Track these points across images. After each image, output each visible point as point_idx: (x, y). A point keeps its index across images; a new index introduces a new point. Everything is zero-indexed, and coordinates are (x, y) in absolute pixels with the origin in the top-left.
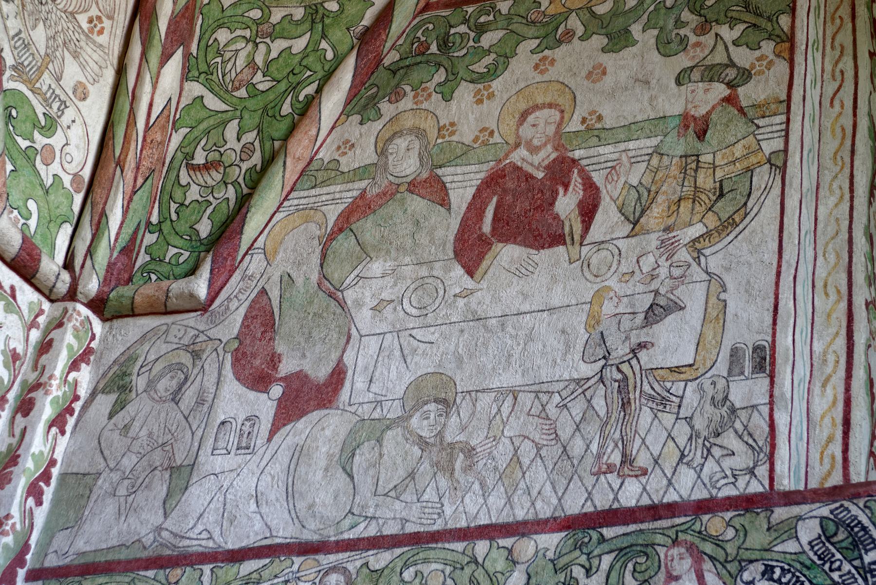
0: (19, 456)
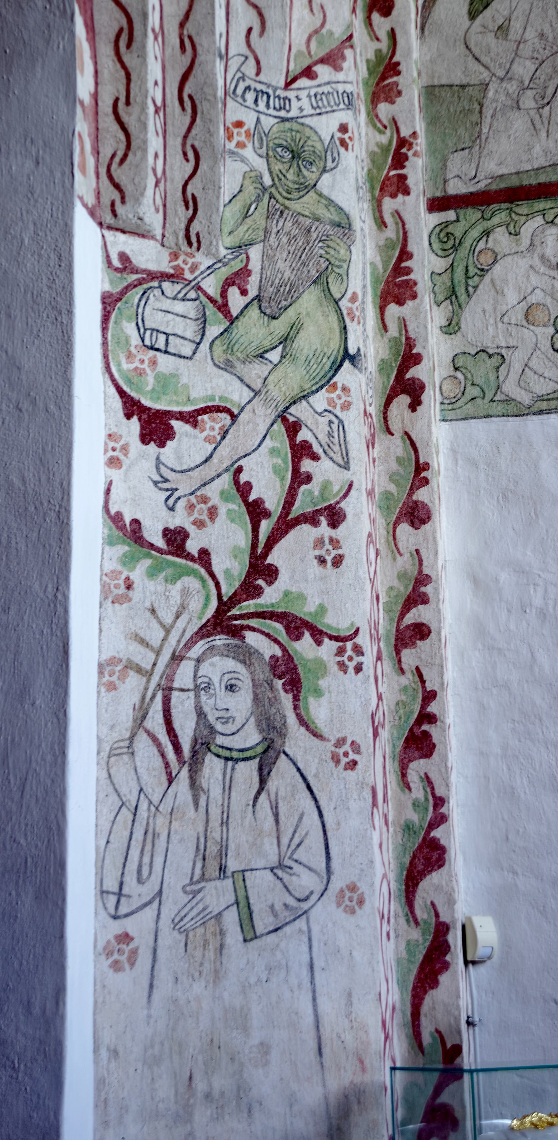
0: (398, 64)
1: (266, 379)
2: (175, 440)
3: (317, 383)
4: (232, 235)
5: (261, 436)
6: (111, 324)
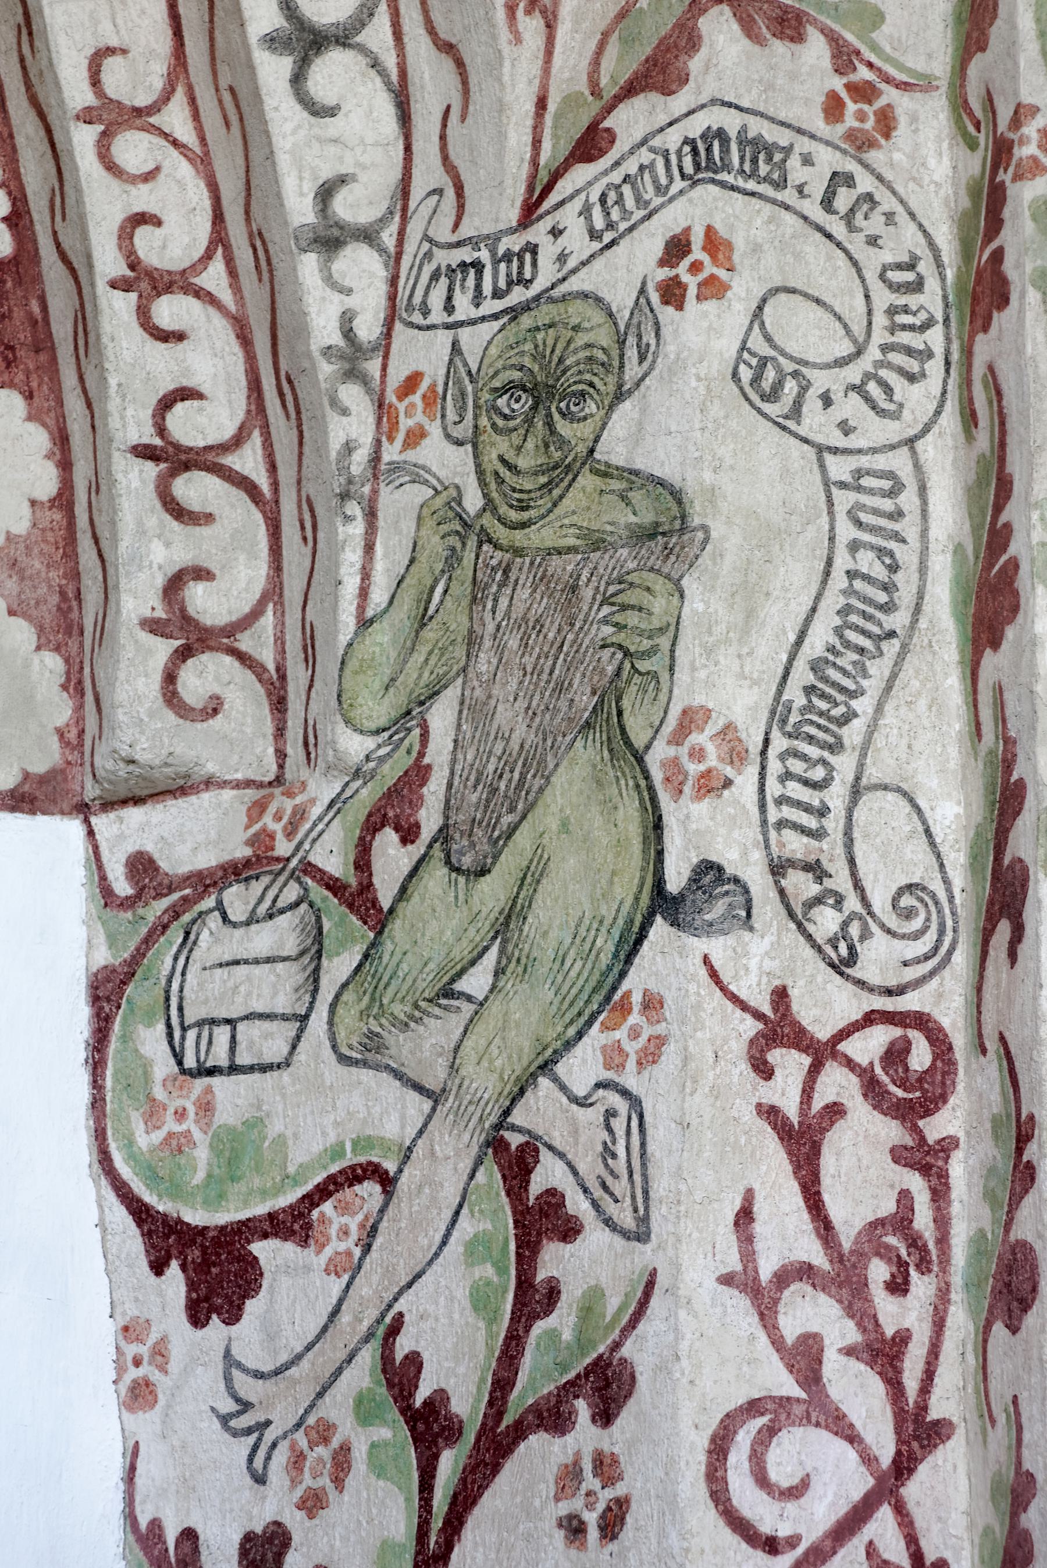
1: (457, 1049)
2: (261, 1294)
3: (579, 1014)
4: (392, 690)
5: (447, 1215)
6: (114, 1045)
